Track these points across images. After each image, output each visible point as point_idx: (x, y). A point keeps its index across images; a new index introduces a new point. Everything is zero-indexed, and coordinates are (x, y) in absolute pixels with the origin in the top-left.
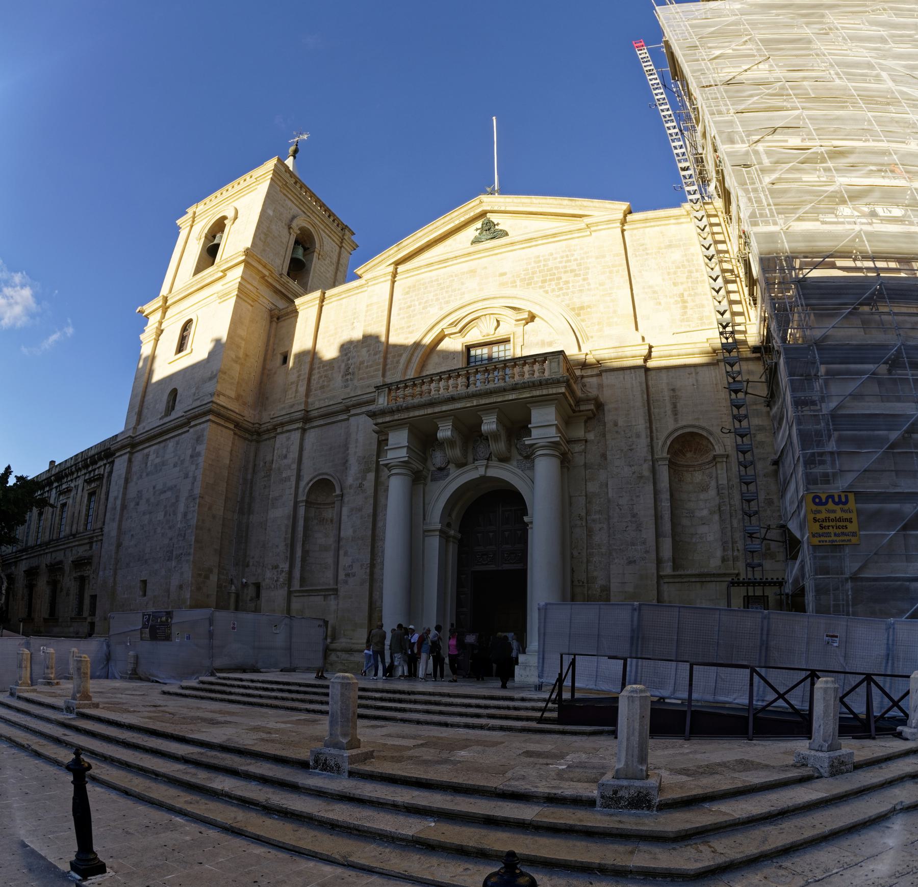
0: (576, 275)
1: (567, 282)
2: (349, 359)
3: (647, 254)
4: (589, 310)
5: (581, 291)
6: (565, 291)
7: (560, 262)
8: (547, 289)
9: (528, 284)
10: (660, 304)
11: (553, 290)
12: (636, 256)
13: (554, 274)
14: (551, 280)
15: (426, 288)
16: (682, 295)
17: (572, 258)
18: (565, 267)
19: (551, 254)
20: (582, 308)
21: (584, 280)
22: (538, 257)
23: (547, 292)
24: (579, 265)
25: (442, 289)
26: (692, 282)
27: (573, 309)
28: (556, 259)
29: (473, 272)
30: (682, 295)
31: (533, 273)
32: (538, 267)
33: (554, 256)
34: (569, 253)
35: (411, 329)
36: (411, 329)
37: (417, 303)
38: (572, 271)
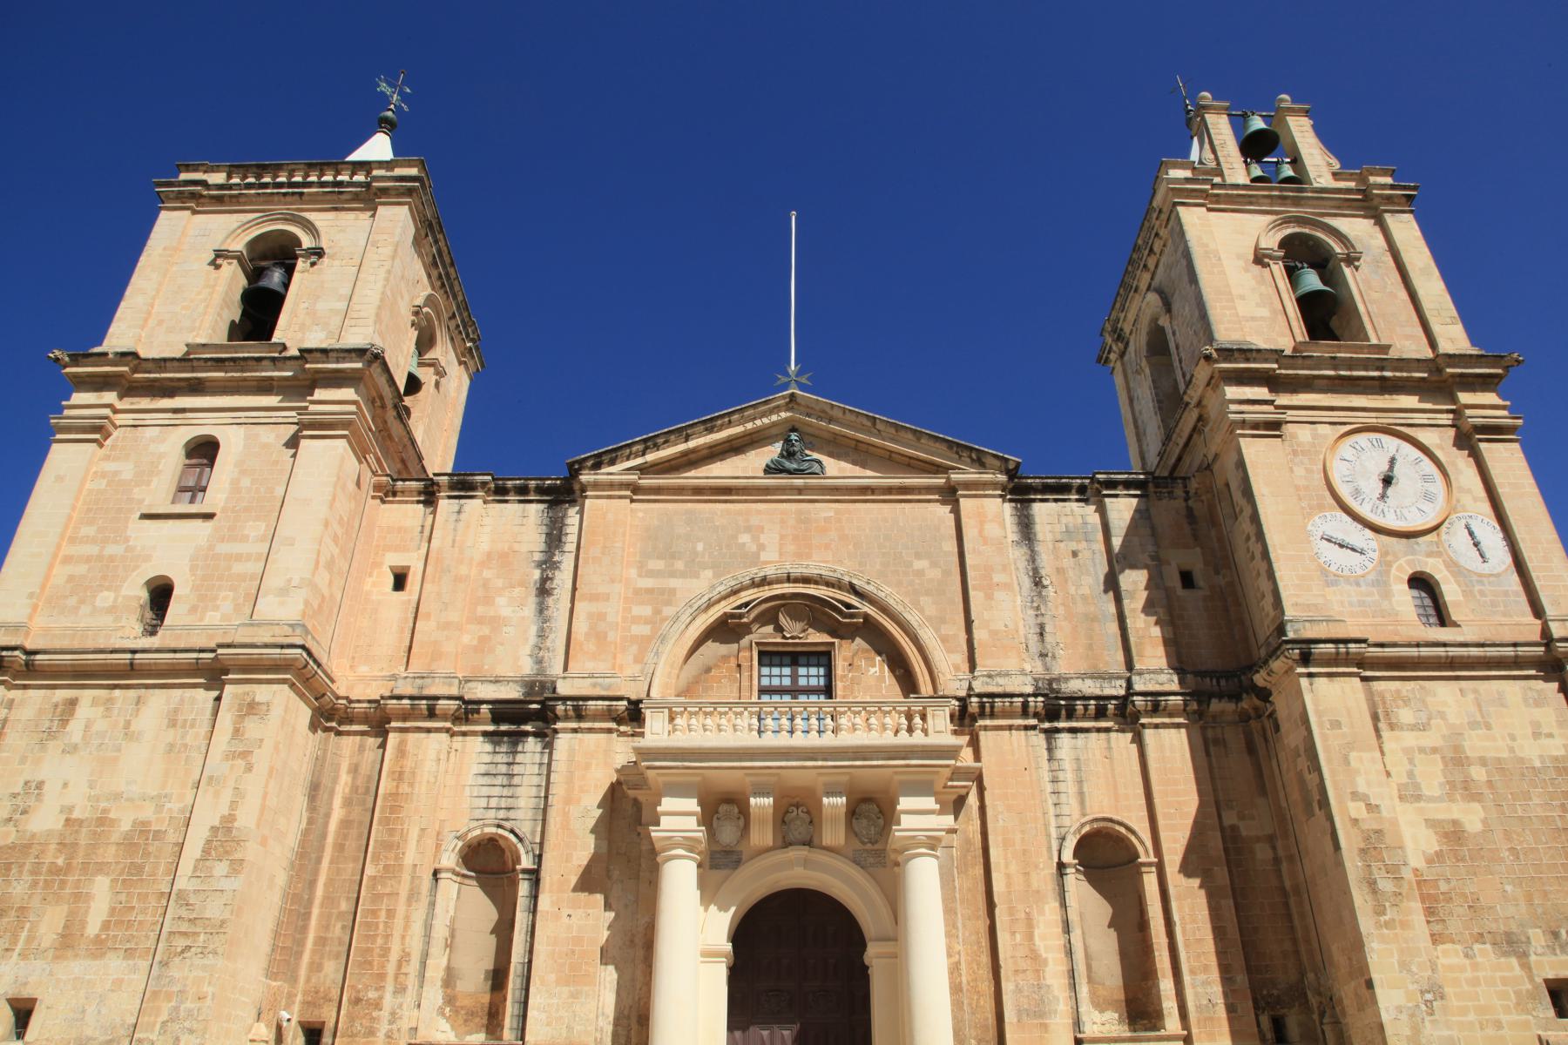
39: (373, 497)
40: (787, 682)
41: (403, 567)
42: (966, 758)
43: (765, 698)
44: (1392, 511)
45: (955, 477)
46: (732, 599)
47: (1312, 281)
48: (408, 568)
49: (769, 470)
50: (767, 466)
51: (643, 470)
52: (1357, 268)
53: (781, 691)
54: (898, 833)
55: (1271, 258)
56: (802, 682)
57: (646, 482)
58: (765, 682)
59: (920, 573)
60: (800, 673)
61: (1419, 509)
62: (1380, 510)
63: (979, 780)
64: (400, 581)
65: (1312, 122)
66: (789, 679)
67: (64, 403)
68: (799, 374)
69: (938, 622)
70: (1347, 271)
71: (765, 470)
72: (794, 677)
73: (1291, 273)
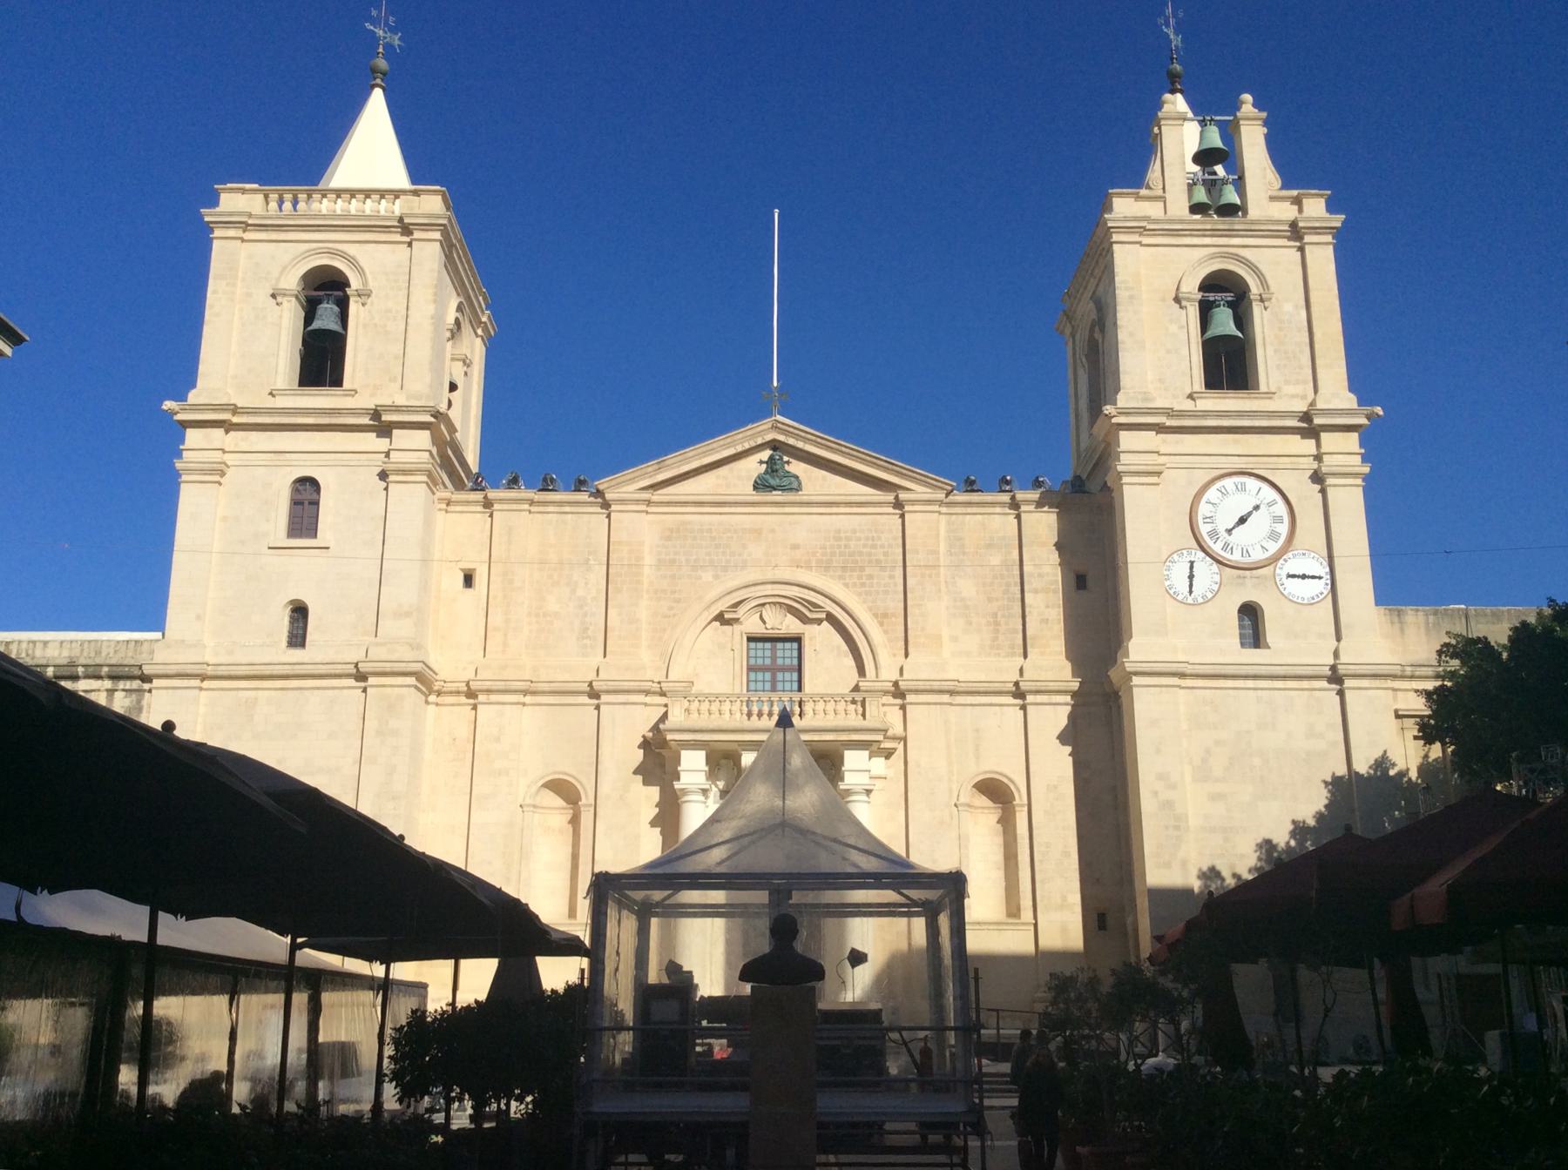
0: (883, 569)
1: (870, 577)
2: (585, 615)
3: (964, 553)
4: (893, 619)
5: (886, 592)
6: (867, 589)
7: (865, 546)
8: (847, 581)
9: (827, 568)
10: (971, 624)
11: (855, 585)
12: (951, 555)
13: (857, 562)
14: (853, 570)
15: (695, 538)
16: (995, 615)
17: (879, 543)
18: (870, 554)
19: (854, 531)
20: (885, 615)
21: (891, 577)
22: (839, 531)
23: (846, 585)
24: (886, 554)
25: (717, 546)
26: (1008, 598)
27: (876, 615)
28: (859, 539)
29: (758, 532)
30: (995, 615)
31: (833, 554)
32: (839, 546)
33: (858, 534)
34: (875, 535)
35: (677, 596)
36: (677, 596)
37: (683, 559)
38: (878, 561)
39: (440, 510)
40: (768, 662)
41: (470, 569)
42: (897, 729)
43: (752, 676)
44: (1240, 548)
45: (903, 496)
46: (728, 597)
47: (1224, 323)
48: (475, 569)
49: (761, 485)
50: (755, 482)
51: (654, 487)
52: (1266, 309)
53: (763, 669)
54: (842, 786)
55: (1188, 300)
56: (780, 662)
57: (657, 496)
58: (752, 661)
59: (870, 577)
60: (778, 655)
61: (1262, 547)
62: (1229, 547)
63: (905, 739)
64: (468, 580)
65: (1265, 130)
66: (770, 651)
67: (181, 447)
68: (780, 388)
69: (882, 617)
70: (1257, 309)
71: (754, 486)
72: (774, 658)
73: (1206, 309)
